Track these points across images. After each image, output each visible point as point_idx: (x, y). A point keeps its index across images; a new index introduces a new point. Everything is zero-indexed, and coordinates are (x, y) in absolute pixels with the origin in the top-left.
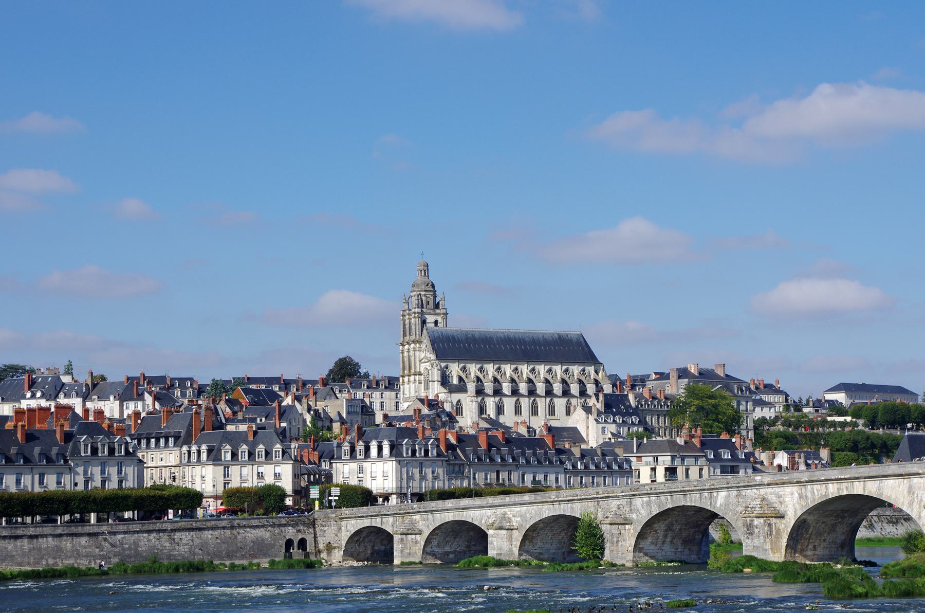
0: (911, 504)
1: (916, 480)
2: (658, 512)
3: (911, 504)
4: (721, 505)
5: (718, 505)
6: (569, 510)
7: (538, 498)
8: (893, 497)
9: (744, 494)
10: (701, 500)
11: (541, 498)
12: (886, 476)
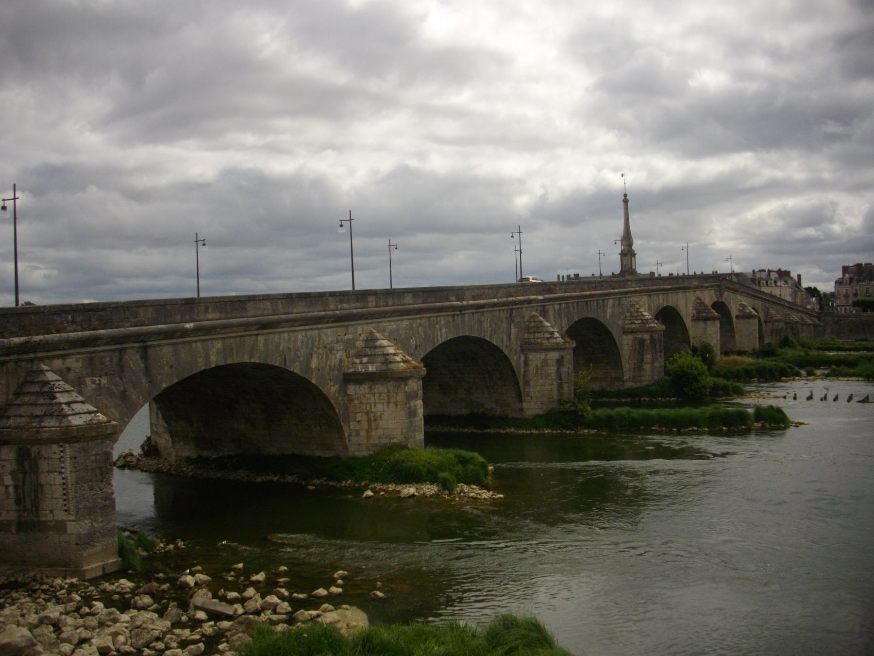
2: (567, 327)
5: (608, 317)
12: (680, 288)
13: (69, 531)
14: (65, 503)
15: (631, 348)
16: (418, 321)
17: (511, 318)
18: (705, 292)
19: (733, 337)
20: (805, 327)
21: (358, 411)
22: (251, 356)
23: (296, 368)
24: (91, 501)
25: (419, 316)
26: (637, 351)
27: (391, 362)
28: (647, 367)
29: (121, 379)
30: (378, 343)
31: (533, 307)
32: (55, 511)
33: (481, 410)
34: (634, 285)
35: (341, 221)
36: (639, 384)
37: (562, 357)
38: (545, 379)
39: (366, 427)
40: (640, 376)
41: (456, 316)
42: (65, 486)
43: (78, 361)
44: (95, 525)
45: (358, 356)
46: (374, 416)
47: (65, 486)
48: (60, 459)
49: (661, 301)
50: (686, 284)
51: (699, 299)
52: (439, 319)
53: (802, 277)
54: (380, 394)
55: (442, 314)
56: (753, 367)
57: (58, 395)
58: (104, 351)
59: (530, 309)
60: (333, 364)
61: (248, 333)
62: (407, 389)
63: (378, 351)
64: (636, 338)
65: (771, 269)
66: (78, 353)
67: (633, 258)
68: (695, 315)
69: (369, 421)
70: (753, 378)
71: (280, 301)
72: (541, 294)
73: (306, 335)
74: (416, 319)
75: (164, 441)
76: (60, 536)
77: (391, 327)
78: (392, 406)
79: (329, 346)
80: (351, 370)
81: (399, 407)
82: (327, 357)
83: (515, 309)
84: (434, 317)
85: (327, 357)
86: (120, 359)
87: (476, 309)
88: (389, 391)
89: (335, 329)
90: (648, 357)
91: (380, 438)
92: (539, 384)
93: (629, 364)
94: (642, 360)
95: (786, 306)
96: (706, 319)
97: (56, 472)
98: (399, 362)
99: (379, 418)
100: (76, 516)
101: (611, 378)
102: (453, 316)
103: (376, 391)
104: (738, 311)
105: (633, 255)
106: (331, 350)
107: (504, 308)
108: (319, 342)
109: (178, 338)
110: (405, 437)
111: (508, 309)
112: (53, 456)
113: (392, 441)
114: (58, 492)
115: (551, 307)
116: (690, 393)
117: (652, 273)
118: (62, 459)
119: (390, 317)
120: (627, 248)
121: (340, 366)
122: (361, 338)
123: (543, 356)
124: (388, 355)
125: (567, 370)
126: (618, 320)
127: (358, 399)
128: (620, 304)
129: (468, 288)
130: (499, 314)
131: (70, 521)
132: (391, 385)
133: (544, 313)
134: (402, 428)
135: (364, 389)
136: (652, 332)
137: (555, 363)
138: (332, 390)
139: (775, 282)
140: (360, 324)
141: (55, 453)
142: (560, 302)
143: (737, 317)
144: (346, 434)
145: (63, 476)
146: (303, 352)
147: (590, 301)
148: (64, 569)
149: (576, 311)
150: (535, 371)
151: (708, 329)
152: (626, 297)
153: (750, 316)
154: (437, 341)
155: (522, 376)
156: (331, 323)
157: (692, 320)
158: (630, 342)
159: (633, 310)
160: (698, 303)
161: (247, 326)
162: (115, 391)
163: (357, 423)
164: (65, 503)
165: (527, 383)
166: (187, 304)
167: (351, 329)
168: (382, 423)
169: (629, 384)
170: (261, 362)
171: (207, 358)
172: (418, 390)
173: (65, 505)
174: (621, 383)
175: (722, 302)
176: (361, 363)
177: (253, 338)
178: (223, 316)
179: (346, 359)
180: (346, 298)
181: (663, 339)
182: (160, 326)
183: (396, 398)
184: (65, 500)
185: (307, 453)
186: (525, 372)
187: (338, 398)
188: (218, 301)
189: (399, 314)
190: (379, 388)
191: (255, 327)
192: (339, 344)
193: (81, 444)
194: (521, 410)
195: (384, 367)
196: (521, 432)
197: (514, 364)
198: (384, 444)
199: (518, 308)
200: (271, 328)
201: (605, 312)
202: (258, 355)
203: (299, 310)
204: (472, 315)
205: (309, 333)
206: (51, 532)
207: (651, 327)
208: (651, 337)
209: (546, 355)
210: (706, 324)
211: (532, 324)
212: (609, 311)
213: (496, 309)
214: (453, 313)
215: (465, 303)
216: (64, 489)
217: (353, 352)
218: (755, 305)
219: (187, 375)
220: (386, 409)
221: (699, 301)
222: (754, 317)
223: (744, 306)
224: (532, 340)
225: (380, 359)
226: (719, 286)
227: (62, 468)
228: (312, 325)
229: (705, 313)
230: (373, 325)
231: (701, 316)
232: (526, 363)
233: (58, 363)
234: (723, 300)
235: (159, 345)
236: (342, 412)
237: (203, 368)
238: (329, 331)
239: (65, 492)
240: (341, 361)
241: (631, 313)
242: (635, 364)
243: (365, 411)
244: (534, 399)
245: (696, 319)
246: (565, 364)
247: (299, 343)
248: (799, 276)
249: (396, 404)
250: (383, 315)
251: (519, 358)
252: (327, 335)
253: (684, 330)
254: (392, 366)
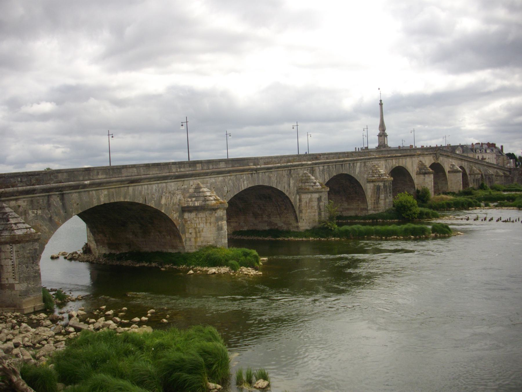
2: (329, 179)
4: (358, 173)
5: (357, 173)
6: (267, 179)
7: (236, 165)
8: (409, 168)
9: (366, 164)
10: (349, 169)
11: (238, 165)
12: (408, 156)
13: (16, 289)
14: (14, 274)
15: (372, 191)
16: (229, 177)
17: (290, 175)
18: (425, 157)
19: (447, 184)
20: (498, 178)
21: (190, 227)
22: (125, 198)
23: (152, 204)
24: (27, 274)
25: (229, 174)
26: (375, 193)
27: (208, 200)
28: (382, 202)
29: (49, 211)
30: (201, 190)
31: (305, 168)
32: (9, 279)
33: (276, 227)
34: (375, 154)
35: (182, 122)
36: (377, 212)
37: (321, 197)
38: (311, 209)
39: (194, 236)
40: (378, 207)
41: (253, 174)
42: (13, 266)
43: (24, 202)
44: (30, 285)
45: (190, 197)
46: (199, 230)
47: (13, 266)
48: (10, 252)
49: (394, 163)
50: (413, 153)
51: (421, 161)
52: (242, 176)
53: (503, 147)
54: (202, 218)
55: (244, 173)
56: (452, 202)
57: (11, 219)
58: (39, 196)
59: (303, 169)
60: (175, 201)
61: (123, 186)
62: (216, 215)
63: (201, 194)
64: (375, 185)
65: (483, 143)
66: (24, 198)
67: (386, 138)
68: (419, 171)
69: (196, 233)
70: (452, 208)
71: (142, 168)
72: (310, 161)
73: (158, 186)
74: (227, 176)
75: (93, 245)
76: (12, 291)
77: (211, 181)
78: (208, 224)
79: (172, 192)
80: (186, 205)
81: (212, 225)
82: (171, 198)
83: (293, 169)
84: (239, 175)
85: (171, 198)
86: (48, 201)
87: (267, 170)
88: (206, 216)
89: (176, 183)
90: (382, 196)
91: (202, 242)
92: (308, 212)
93: (371, 200)
94: (379, 198)
95: (485, 165)
96: (425, 174)
97: (9, 259)
98: (212, 200)
99: (201, 231)
100: (19, 281)
101: (361, 208)
102: (252, 174)
103: (200, 216)
104: (449, 168)
105: (386, 136)
106: (174, 194)
107: (285, 169)
108: (166, 190)
109: (81, 189)
110: (216, 242)
111: (288, 170)
112: (7, 250)
113: (209, 244)
114: (10, 269)
115: (317, 168)
116: (406, 217)
117: (411, 146)
118: (12, 252)
119: (211, 175)
120: (382, 132)
121: (180, 203)
122: (192, 187)
123: (309, 196)
124: (206, 196)
125: (323, 204)
126: (364, 175)
127: (190, 221)
128: (365, 165)
129: (262, 158)
130: (282, 172)
131: (16, 284)
132: (207, 213)
133: (313, 172)
134: (214, 237)
135: (193, 215)
136: (384, 181)
137: (316, 200)
138: (174, 216)
139: (486, 150)
140: (191, 180)
141: (8, 249)
142: (323, 165)
143: (449, 172)
144: (184, 240)
145: (12, 261)
146: (156, 195)
147: (344, 164)
148: (13, 308)
149: (334, 170)
150: (305, 204)
151: (426, 179)
152: (369, 161)
153: (457, 171)
154: (241, 189)
155: (298, 208)
156: (173, 179)
157: (416, 174)
158: (372, 187)
159: (373, 169)
160: (420, 164)
161: (122, 182)
162: (46, 217)
163: (189, 234)
164: (14, 274)
165: (301, 212)
166: (87, 171)
167: (186, 182)
168: (203, 234)
169: (371, 212)
170: (131, 201)
171: (99, 199)
172: (223, 216)
173: (14, 276)
174: (367, 211)
175: (438, 163)
176: (191, 201)
177: (126, 188)
178: (108, 176)
179: (183, 199)
180: (183, 165)
181: (391, 186)
182: (70, 183)
183: (210, 220)
184: (13, 273)
185: (165, 250)
186: (299, 205)
187: (178, 220)
188: (104, 168)
189: (216, 174)
190: (201, 215)
191: (127, 182)
192: (179, 191)
193: (21, 244)
194: (298, 227)
195: (204, 203)
196: (297, 239)
197: (292, 201)
198: (205, 245)
199: (295, 169)
200: (136, 183)
201: (355, 170)
202: (129, 197)
203: (153, 173)
204: (264, 173)
205: (160, 185)
206: (7, 290)
207: (384, 179)
208: (384, 184)
209: (311, 196)
210: (425, 176)
211: (304, 178)
212: (357, 170)
213: (280, 169)
214: (252, 172)
215: (259, 167)
216: (13, 267)
217: (188, 195)
218: (462, 164)
219: (87, 208)
220: (205, 226)
221: (421, 163)
222: (459, 172)
223: (453, 166)
224: (303, 187)
225: (202, 199)
226: (435, 154)
227: (12, 256)
228: (162, 180)
229: (424, 170)
230: (199, 180)
231: (422, 171)
232: (300, 200)
233: (13, 203)
234: (439, 162)
235: (70, 193)
236: (181, 228)
237: (96, 205)
238: (172, 184)
239: (13, 269)
240: (180, 200)
241: (372, 170)
242: (374, 200)
243: (194, 227)
244: (305, 221)
245: (419, 173)
246: (323, 200)
247: (154, 191)
248: (502, 147)
249: (210, 223)
250: (206, 174)
251: (296, 198)
252: (171, 186)
253: (411, 180)
254: (208, 203)
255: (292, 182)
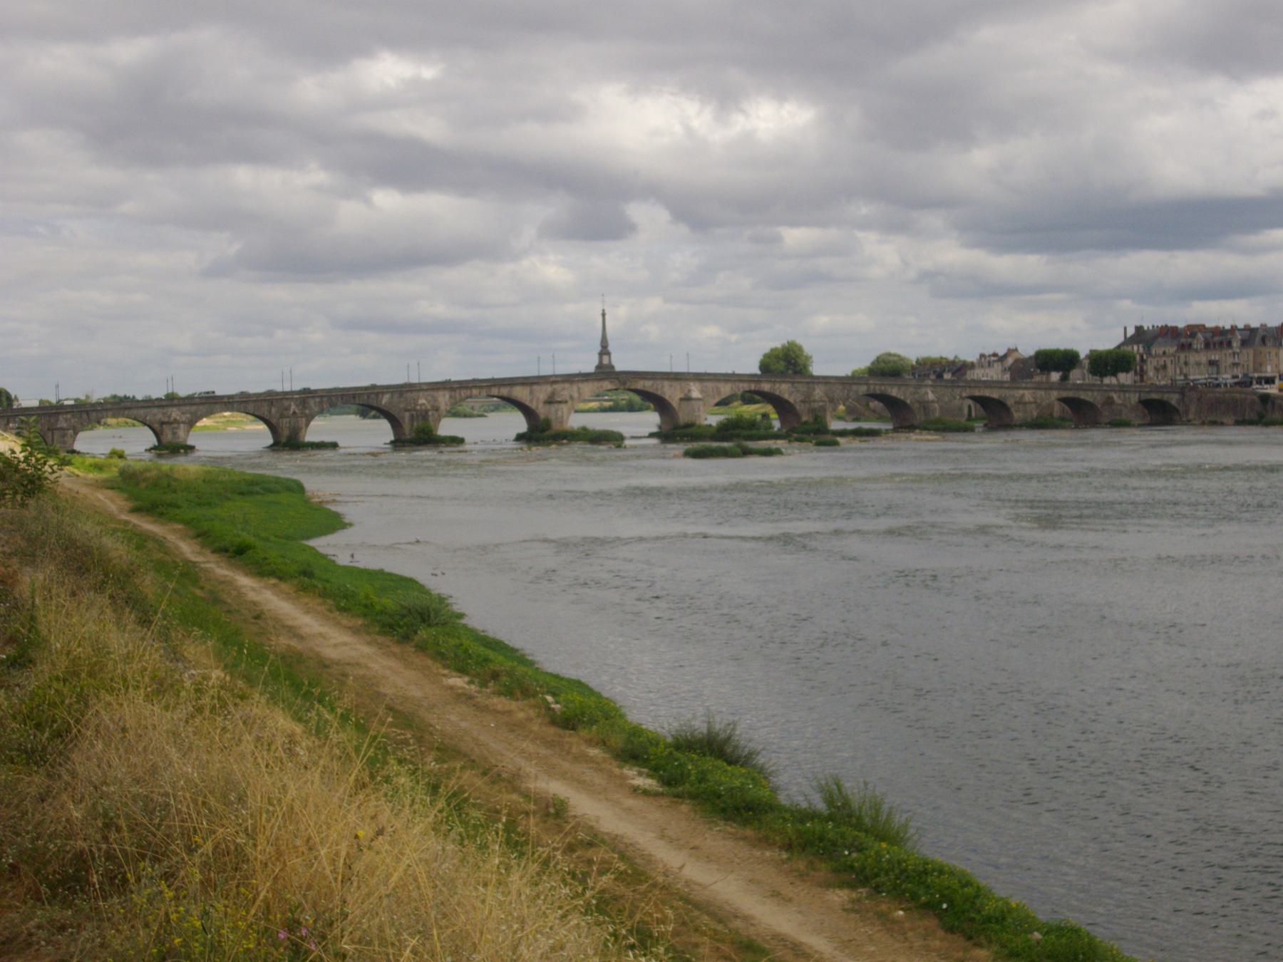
0: (531, 401)
1: (535, 387)
3: (531, 401)
5: (383, 402)
20: (1021, 406)
143: (681, 399)
255: (273, 410)
